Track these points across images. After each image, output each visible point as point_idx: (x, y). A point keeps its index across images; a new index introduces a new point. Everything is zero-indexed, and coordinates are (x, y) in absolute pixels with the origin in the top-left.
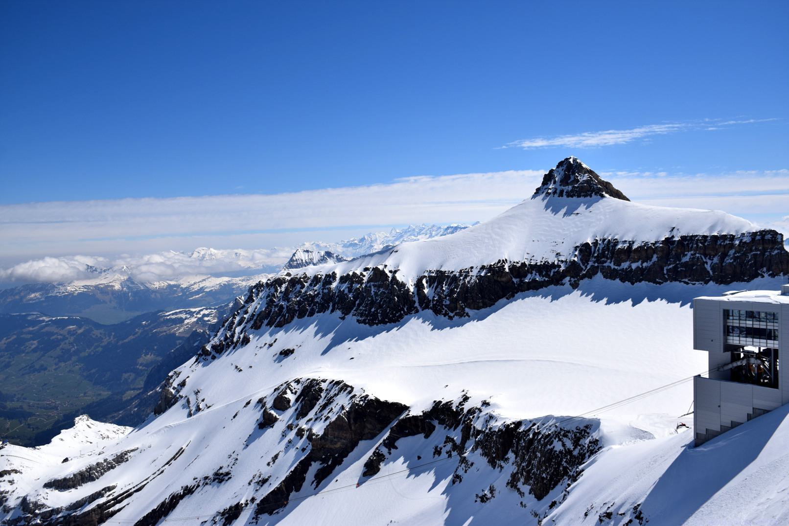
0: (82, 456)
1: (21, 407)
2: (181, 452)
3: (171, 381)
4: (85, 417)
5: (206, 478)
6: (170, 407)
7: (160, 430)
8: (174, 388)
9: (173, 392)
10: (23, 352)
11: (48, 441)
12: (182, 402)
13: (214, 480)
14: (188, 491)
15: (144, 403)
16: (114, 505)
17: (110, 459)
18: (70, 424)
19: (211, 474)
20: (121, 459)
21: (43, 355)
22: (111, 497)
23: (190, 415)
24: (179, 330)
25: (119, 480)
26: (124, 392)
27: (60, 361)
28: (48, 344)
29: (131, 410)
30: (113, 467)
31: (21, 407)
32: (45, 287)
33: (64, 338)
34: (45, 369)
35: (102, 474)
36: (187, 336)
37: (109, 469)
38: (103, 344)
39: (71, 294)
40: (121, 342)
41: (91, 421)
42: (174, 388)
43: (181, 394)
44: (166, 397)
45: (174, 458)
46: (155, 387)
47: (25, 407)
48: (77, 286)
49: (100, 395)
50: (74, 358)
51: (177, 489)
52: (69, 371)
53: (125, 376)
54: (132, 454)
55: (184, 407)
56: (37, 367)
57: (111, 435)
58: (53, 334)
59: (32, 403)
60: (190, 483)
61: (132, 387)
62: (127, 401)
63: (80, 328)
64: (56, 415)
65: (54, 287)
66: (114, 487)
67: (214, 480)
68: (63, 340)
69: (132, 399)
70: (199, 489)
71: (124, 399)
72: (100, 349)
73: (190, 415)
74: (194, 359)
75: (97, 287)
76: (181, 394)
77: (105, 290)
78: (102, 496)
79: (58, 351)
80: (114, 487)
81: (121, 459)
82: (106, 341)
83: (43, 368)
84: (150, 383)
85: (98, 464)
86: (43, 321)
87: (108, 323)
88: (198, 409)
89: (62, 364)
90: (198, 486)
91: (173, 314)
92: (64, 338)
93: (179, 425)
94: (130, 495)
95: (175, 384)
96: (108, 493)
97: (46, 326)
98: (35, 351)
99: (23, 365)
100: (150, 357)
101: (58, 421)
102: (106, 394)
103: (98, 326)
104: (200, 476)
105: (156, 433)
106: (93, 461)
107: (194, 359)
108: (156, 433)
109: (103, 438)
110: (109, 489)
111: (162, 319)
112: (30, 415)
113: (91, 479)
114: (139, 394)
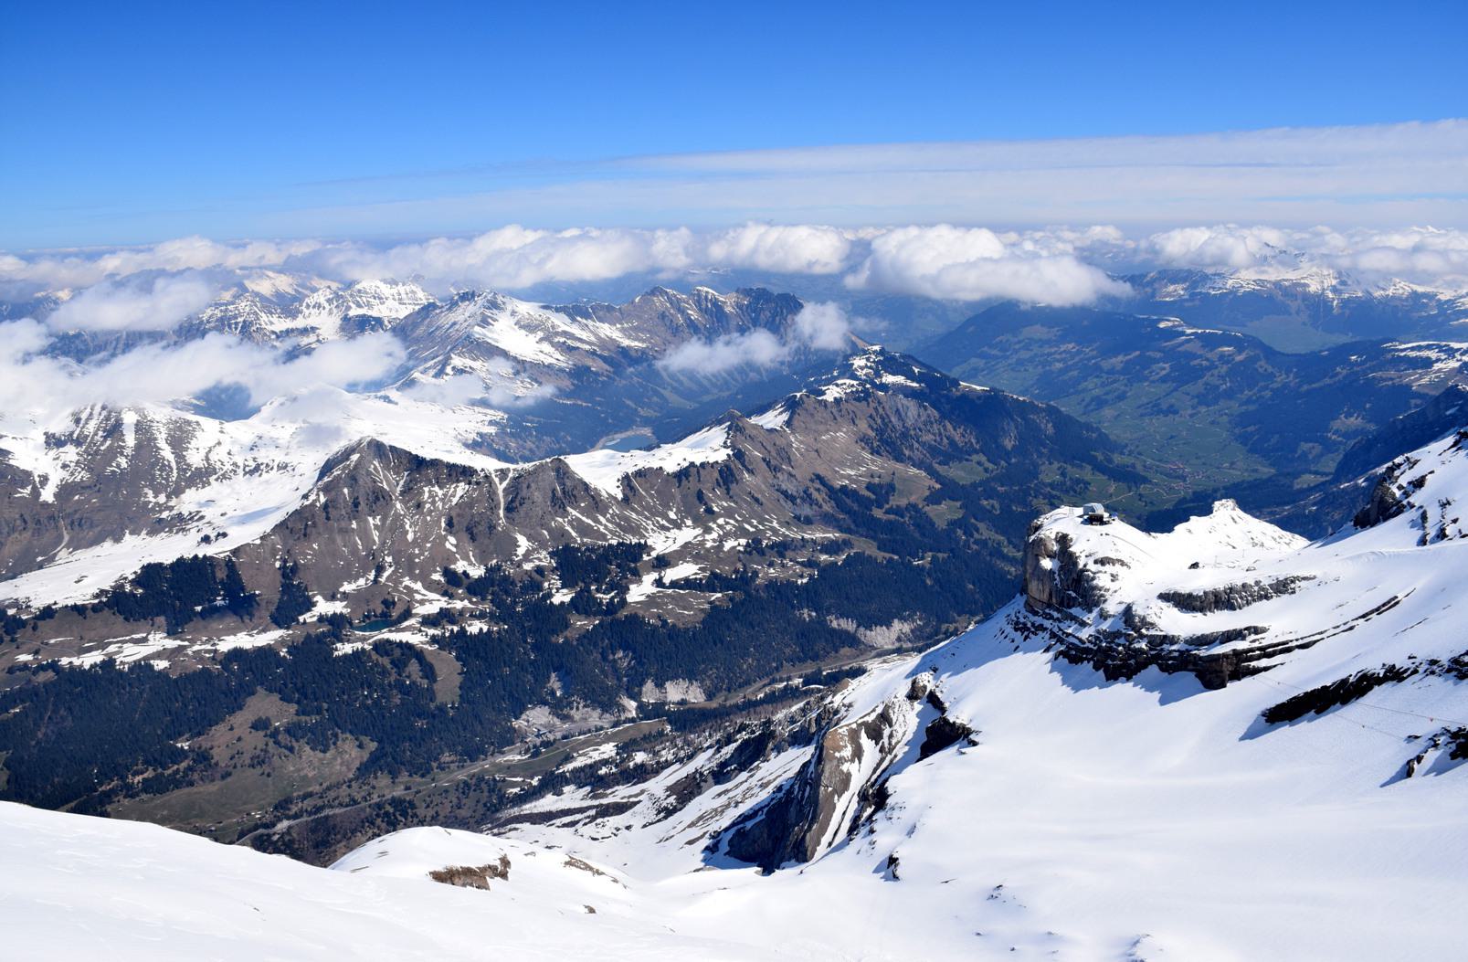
0: (1217, 565)
1: (1133, 466)
2: (1392, 603)
3: (1397, 473)
4: (1230, 503)
5: (1433, 662)
6: (1385, 519)
7: (1359, 556)
8: (1400, 487)
9: (1398, 494)
10: (1146, 379)
11: (1170, 530)
12: (1412, 514)
13: (1449, 671)
14: (1395, 674)
15: (1329, 501)
16: (1259, 658)
17: (1266, 582)
18: (1206, 511)
19: (1445, 659)
20: (1283, 587)
21: (1176, 389)
22: (1256, 645)
23: (1423, 542)
24: (1420, 381)
25: (1276, 620)
26: (1297, 475)
27: (1200, 403)
28: (1186, 371)
29: (1305, 507)
30: (1267, 597)
31: (1133, 466)
32: (1193, 276)
33: (1213, 366)
34: (1176, 412)
35: (1248, 603)
36: (1436, 393)
37: (1261, 598)
38: (1275, 386)
39: (1233, 292)
40: (1305, 387)
41: (1239, 512)
42: (1400, 487)
43: (1411, 499)
44: (1382, 501)
45: (1378, 610)
46: (1356, 477)
47: (1139, 467)
48: (1246, 279)
49: (1255, 471)
50: (1222, 403)
51: (1375, 666)
52: (1213, 423)
53: (1305, 446)
54: (1303, 584)
55: (1413, 524)
56: (1164, 407)
57: (1269, 543)
58: (1195, 356)
59: (1149, 461)
60: (1401, 662)
61: (1313, 468)
62: (1302, 491)
63: (1240, 352)
64: (1182, 490)
65: (1205, 278)
66: (1264, 630)
67: (1449, 671)
68: (1208, 369)
69: (1311, 490)
70: (1416, 677)
71: (1296, 487)
72: (1268, 394)
73: (1423, 542)
74: (1450, 440)
75: (1277, 284)
76: (1411, 499)
77: (1292, 292)
78: (1244, 638)
79: (1198, 387)
80: (1264, 630)
81: (1283, 587)
82: (1281, 379)
83: (1172, 410)
84: (1348, 467)
85: (1244, 586)
86: (1183, 333)
87: (1289, 350)
88: (1442, 535)
89: (1203, 409)
90: (1415, 672)
91: (1412, 349)
92: (1213, 366)
93: (1398, 555)
94: (1289, 650)
95: (1403, 481)
96: (1253, 637)
97: (1188, 341)
98: (1164, 380)
99: (1145, 400)
100: (1354, 422)
101: (1183, 500)
102: (1266, 471)
103: (1270, 353)
104: (1423, 654)
105: (1351, 558)
106: (1237, 579)
107: (1450, 440)
108: (1351, 558)
109: (1255, 545)
110: (1256, 630)
111: (1389, 356)
112: (1145, 480)
113: (1232, 608)
114: (1323, 483)
